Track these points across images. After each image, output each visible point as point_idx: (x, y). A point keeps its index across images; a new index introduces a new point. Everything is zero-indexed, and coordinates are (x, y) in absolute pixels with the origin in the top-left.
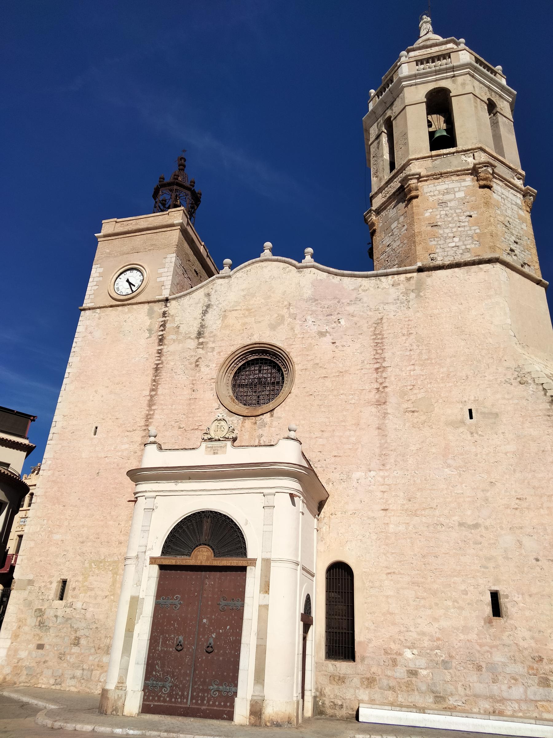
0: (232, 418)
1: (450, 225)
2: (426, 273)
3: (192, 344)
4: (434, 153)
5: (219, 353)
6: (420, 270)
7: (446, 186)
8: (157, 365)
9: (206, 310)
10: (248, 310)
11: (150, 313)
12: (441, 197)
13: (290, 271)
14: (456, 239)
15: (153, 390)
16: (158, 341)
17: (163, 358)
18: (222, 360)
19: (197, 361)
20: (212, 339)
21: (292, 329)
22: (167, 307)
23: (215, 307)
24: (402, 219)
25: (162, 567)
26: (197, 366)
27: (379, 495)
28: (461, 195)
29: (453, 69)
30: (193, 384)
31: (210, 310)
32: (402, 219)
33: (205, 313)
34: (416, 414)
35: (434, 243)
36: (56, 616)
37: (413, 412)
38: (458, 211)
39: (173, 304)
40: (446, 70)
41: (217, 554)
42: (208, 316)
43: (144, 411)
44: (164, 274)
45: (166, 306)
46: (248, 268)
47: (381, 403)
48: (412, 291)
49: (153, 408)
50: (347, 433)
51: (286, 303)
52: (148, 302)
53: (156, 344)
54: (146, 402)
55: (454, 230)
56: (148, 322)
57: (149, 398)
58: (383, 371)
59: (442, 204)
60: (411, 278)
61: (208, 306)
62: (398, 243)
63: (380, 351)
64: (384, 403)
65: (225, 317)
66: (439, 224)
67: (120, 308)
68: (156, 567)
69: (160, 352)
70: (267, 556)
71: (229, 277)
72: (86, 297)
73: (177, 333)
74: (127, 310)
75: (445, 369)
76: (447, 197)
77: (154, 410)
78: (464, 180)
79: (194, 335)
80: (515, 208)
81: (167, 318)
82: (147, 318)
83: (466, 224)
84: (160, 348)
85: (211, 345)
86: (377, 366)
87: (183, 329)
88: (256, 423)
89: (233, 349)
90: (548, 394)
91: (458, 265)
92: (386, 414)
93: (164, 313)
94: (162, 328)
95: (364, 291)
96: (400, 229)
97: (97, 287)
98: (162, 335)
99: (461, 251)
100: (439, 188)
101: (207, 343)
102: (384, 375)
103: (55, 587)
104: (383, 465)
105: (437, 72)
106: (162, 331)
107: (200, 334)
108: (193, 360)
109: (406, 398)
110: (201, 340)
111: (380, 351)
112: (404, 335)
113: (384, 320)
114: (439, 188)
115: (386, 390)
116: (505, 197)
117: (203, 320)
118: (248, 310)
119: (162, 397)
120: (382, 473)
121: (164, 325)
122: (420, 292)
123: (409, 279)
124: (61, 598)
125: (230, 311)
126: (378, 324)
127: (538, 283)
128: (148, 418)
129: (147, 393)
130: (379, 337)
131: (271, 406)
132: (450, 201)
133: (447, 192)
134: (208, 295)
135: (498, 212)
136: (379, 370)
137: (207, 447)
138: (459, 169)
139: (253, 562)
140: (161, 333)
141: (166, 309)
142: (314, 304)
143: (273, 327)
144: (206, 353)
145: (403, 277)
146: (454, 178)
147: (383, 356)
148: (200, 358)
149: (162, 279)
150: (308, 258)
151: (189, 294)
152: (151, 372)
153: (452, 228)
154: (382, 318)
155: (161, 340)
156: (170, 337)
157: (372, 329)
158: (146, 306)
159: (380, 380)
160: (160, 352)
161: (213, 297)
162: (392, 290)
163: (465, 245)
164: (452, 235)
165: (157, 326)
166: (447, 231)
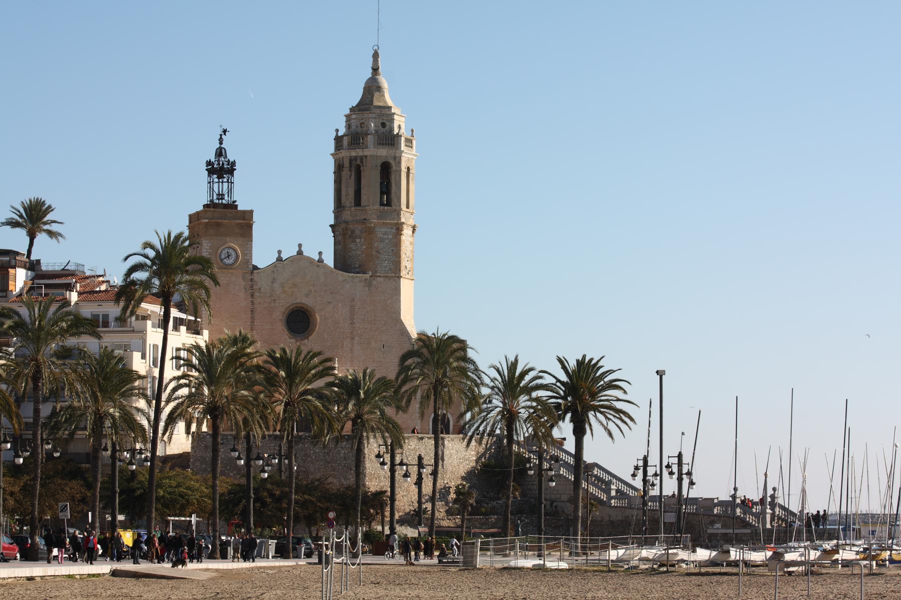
2: (373, 278)
5: (282, 306)
7: (385, 230)
8: (252, 309)
11: (244, 278)
12: (382, 235)
14: (386, 262)
15: (251, 322)
17: (254, 306)
18: (283, 310)
28: (390, 237)
32: (363, 240)
33: (272, 282)
35: (377, 262)
42: (275, 285)
45: (252, 275)
47: (353, 339)
48: (367, 286)
50: (339, 351)
55: (386, 256)
56: (244, 283)
59: (382, 240)
61: (274, 279)
62: (360, 253)
65: (283, 287)
69: (252, 302)
73: (260, 292)
76: (386, 237)
78: (393, 229)
83: (391, 254)
85: (277, 301)
86: (351, 321)
87: (262, 290)
89: (289, 305)
93: (251, 279)
94: (251, 288)
96: (362, 246)
99: (387, 269)
100: (382, 230)
101: (275, 300)
102: (354, 326)
106: (252, 290)
112: (362, 308)
114: (382, 230)
119: (257, 327)
123: (366, 280)
129: (249, 324)
130: (353, 307)
132: (386, 239)
140: (251, 291)
141: (252, 277)
143: (307, 296)
147: (354, 317)
152: (250, 313)
155: (252, 296)
156: (257, 294)
160: (252, 302)
163: (390, 266)
164: (384, 259)
166: (383, 256)
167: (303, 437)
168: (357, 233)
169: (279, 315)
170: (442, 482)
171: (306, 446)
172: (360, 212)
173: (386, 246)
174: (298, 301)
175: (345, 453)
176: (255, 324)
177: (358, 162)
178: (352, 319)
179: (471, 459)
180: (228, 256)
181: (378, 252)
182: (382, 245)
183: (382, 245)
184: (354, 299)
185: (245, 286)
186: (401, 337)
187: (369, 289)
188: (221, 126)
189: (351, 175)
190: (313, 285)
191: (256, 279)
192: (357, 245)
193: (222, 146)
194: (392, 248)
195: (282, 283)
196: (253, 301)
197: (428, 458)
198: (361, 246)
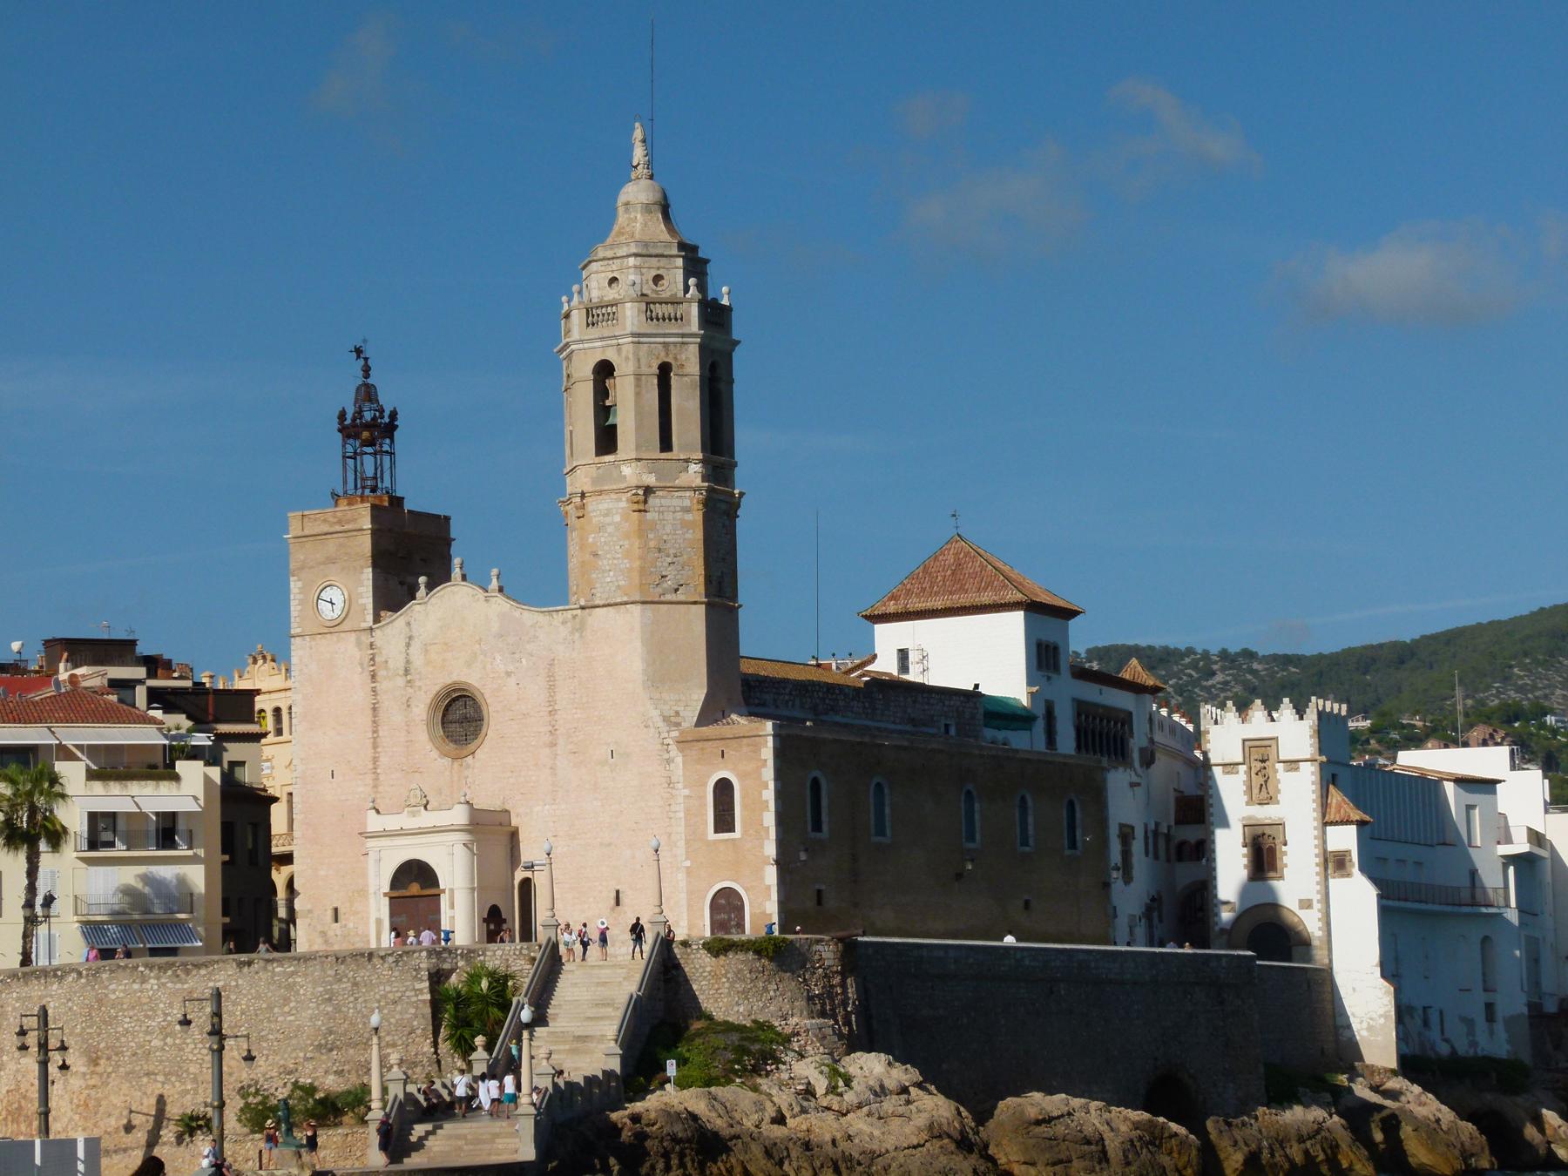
0: (443, 761)
1: (608, 556)
2: (587, 610)
3: (400, 681)
4: (597, 460)
5: (426, 692)
6: (583, 608)
7: (606, 506)
8: (374, 704)
9: (409, 643)
10: (446, 644)
11: (359, 643)
14: (611, 573)
15: (374, 732)
16: (370, 677)
17: (378, 697)
18: (429, 701)
19: (408, 701)
20: (418, 676)
21: (484, 668)
22: (373, 637)
23: (416, 640)
25: (391, 898)
26: (409, 706)
27: (552, 824)
30: (408, 725)
31: (412, 643)
33: (408, 645)
34: (577, 755)
35: (594, 576)
36: (337, 935)
37: (575, 753)
39: (378, 633)
43: (370, 752)
44: (364, 595)
46: (442, 593)
47: (553, 745)
48: (577, 630)
49: (379, 750)
50: (530, 773)
51: (477, 638)
52: (355, 631)
53: (369, 681)
54: (371, 745)
55: (610, 562)
57: (372, 740)
58: (554, 715)
59: (601, 528)
60: (576, 615)
63: (552, 694)
64: (555, 745)
66: (600, 553)
67: (328, 636)
68: (387, 899)
69: (374, 690)
70: (451, 887)
71: (425, 603)
72: (292, 619)
74: (335, 639)
75: (596, 713)
76: (608, 520)
77: (379, 753)
78: (620, 500)
79: (402, 672)
80: (679, 515)
81: (375, 651)
82: (356, 649)
83: (620, 556)
84: (373, 685)
85: (418, 683)
86: (551, 708)
87: (391, 664)
88: (462, 765)
89: (438, 688)
92: (557, 755)
93: (372, 644)
94: (372, 663)
95: (540, 627)
98: (373, 671)
99: (613, 589)
103: (330, 913)
104: (554, 800)
106: (372, 665)
107: (407, 672)
108: (405, 699)
109: (571, 740)
110: (409, 677)
111: (552, 694)
112: (570, 678)
113: (556, 662)
114: (600, 507)
115: (558, 732)
116: (665, 509)
117: (407, 654)
120: (554, 807)
121: (373, 659)
122: (582, 632)
123: (574, 617)
124: (336, 921)
125: (431, 645)
126: (551, 665)
127: (695, 603)
128: (375, 760)
129: (370, 735)
130: (552, 679)
131: (472, 747)
132: (609, 524)
133: (608, 513)
134: (409, 624)
135: (651, 536)
136: (553, 713)
137: (408, 812)
138: (615, 488)
139: (444, 891)
140: (372, 668)
141: (372, 640)
142: (501, 640)
144: (415, 691)
146: (614, 496)
148: (410, 698)
151: (391, 622)
152: (370, 712)
153: (609, 559)
154: (553, 660)
156: (381, 673)
157: (547, 671)
158: (353, 634)
159: (553, 723)
160: (374, 690)
161: (414, 626)
162: (562, 628)
164: (608, 568)
165: (367, 659)
166: (605, 562)
169: (421, 709)
170: (302, 1055)
173: (610, 539)
174: (455, 678)
176: (380, 735)
178: (551, 702)
179: (414, 999)
181: (596, 555)
182: (603, 539)
183: (603, 539)
184: (553, 660)
185: (361, 659)
187: (581, 636)
190: (479, 642)
191: (378, 643)
193: (370, 381)
194: (621, 543)
195: (425, 645)
196: (375, 687)
197: (264, 1006)
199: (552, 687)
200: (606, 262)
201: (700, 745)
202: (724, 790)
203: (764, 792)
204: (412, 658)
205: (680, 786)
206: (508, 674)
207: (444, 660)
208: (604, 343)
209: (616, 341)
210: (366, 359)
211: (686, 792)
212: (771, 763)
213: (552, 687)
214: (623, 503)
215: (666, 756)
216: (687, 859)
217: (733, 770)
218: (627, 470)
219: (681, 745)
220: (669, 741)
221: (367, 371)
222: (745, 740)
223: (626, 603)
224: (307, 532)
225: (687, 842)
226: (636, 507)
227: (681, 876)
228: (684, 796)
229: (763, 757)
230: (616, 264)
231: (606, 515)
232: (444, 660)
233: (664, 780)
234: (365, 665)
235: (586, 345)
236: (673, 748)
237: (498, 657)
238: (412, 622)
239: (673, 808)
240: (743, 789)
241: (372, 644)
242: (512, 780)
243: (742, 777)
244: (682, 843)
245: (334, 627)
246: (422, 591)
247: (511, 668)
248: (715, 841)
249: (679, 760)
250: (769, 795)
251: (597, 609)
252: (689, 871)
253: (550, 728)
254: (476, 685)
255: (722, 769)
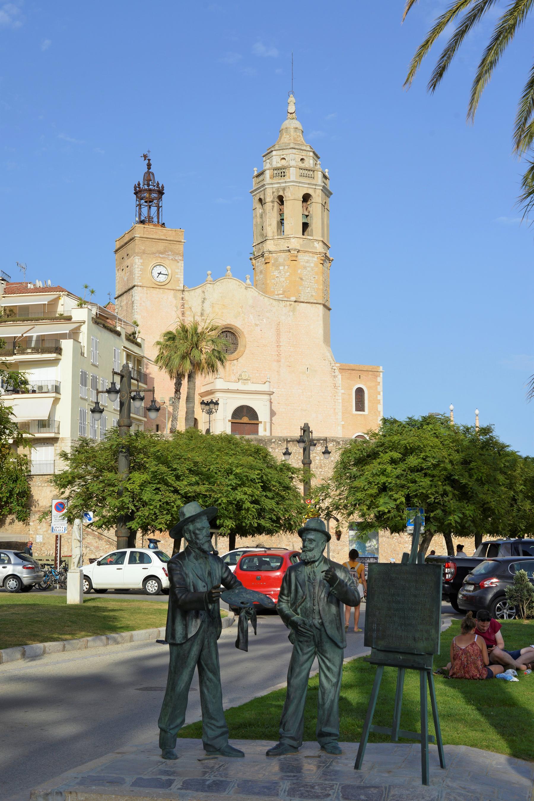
2: (297, 303)
6: (295, 302)
7: (307, 258)
10: (224, 305)
11: (175, 297)
13: (241, 287)
14: (309, 289)
21: (244, 320)
24: (286, 267)
25: (232, 423)
29: (316, 185)
31: (206, 301)
32: (286, 267)
33: (203, 302)
35: (300, 288)
38: (311, 274)
39: (186, 293)
40: (313, 185)
41: (250, 420)
42: (205, 305)
45: (183, 294)
47: (279, 361)
59: (305, 268)
61: (204, 299)
62: (284, 279)
65: (213, 307)
67: (158, 289)
76: (307, 265)
78: (314, 257)
79: (199, 314)
84: (183, 318)
86: (278, 344)
90: (332, 365)
91: (309, 303)
93: (182, 298)
97: (141, 272)
105: (309, 184)
107: (202, 315)
110: (203, 318)
118: (224, 305)
123: (291, 305)
134: (204, 292)
139: (261, 422)
140: (182, 310)
141: (183, 296)
145: (288, 303)
146: (311, 255)
149: (179, 276)
150: (248, 281)
158: (172, 291)
165: (179, 305)
166: (306, 283)
167: (273, 440)
168: (281, 260)
171: (277, 450)
172: (284, 241)
175: (320, 460)
177: (281, 193)
178: (278, 341)
180: (160, 274)
186: (324, 361)
187: (294, 314)
188: (149, 151)
189: (273, 206)
190: (242, 307)
192: (280, 272)
198: (285, 273)
199: (278, 335)
200: (299, 151)
201: (349, 371)
202: (360, 392)
203: (378, 396)
204: (204, 308)
205: (340, 388)
206: (257, 325)
207: (222, 313)
208: (309, 186)
209: (314, 187)
210: (149, 160)
211: (343, 391)
212: (381, 384)
213: (278, 335)
214: (316, 259)
215: (334, 374)
216: (343, 421)
217: (364, 385)
218: (316, 244)
219: (341, 371)
220: (336, 368)
221: (149, 165)
222: (370, 373)
223: (317, 303)
224: (145, 236)
225: (343, 413)
226: (322, 262)
227: (340, 428)
228: (342, 393)
229: (378, 381)
230: (304, 153)
231: (307, 262)
232: (222, 313)
233: (332, 385)
234: (179, 308)
235: (300, 185)
236: (337, 371)
237: (251, 317)
238: (206, 291)
239: (337, 398)
240: (369, 393)
241: (182, 298)
242: (257, 375)
243: (369, 388)
244: (340, 414)
245: (160, 286)
246: (209, 278)
247: (258, 323)
248: (356, 414)
249: (340, 377)
250: (380, 397)
251: (302, 304)
252: (343, 426)
253: (277, 353)
254: (238, 326)
255: (359, 383)
